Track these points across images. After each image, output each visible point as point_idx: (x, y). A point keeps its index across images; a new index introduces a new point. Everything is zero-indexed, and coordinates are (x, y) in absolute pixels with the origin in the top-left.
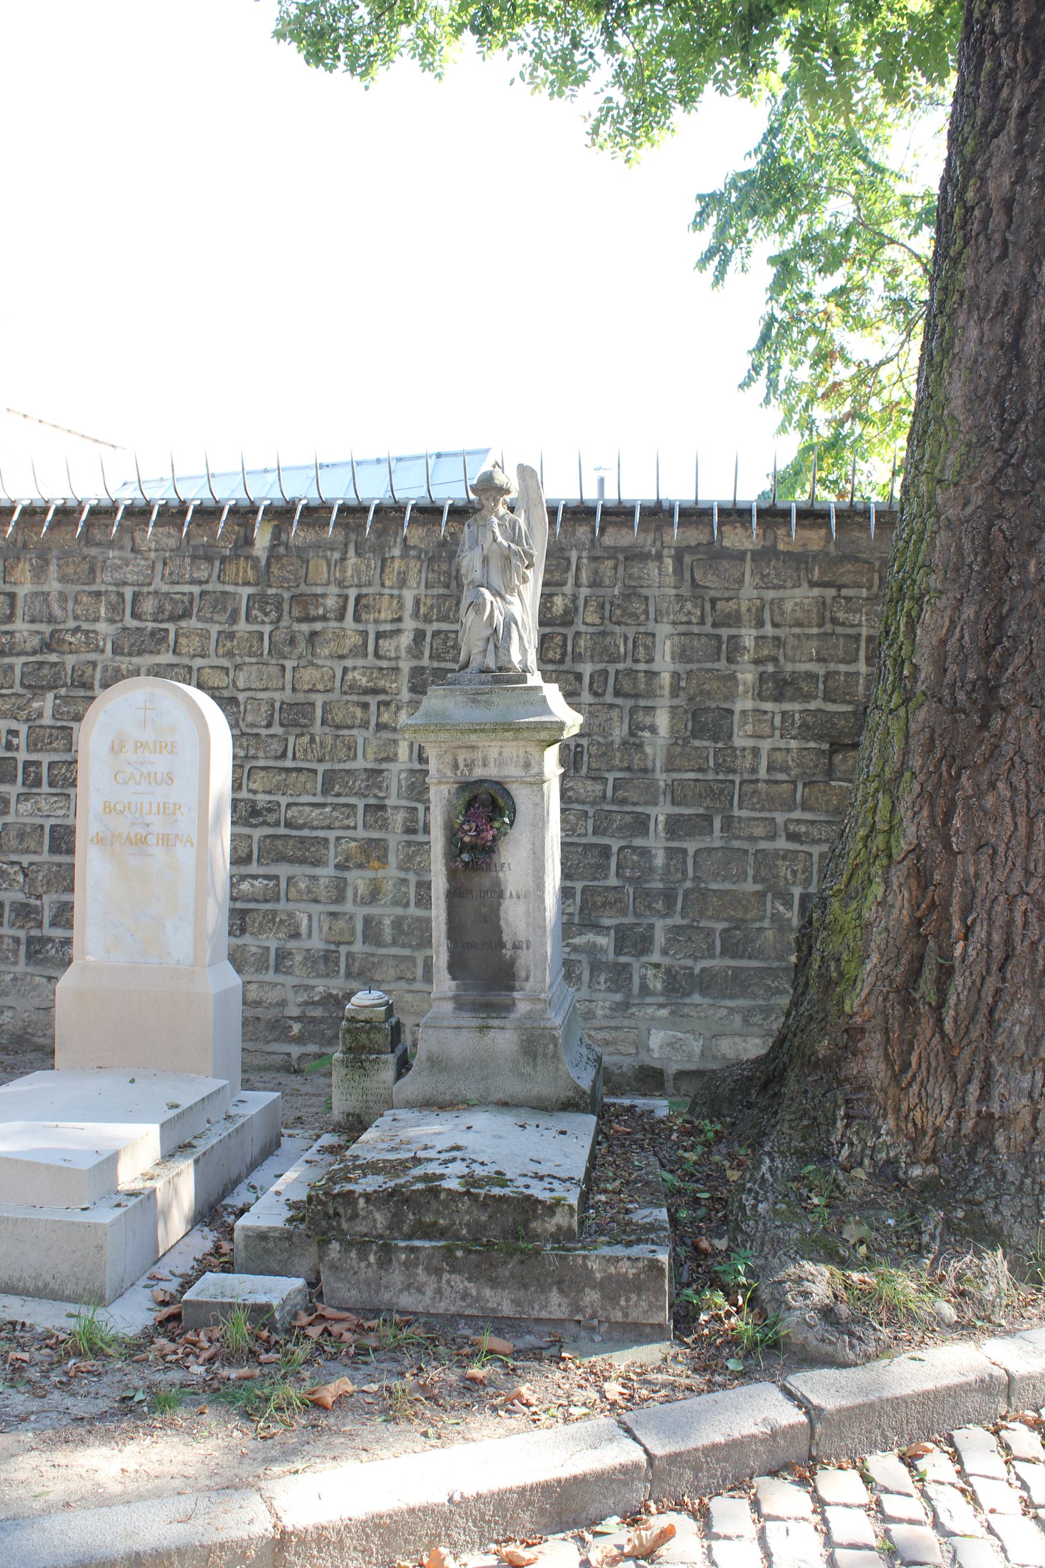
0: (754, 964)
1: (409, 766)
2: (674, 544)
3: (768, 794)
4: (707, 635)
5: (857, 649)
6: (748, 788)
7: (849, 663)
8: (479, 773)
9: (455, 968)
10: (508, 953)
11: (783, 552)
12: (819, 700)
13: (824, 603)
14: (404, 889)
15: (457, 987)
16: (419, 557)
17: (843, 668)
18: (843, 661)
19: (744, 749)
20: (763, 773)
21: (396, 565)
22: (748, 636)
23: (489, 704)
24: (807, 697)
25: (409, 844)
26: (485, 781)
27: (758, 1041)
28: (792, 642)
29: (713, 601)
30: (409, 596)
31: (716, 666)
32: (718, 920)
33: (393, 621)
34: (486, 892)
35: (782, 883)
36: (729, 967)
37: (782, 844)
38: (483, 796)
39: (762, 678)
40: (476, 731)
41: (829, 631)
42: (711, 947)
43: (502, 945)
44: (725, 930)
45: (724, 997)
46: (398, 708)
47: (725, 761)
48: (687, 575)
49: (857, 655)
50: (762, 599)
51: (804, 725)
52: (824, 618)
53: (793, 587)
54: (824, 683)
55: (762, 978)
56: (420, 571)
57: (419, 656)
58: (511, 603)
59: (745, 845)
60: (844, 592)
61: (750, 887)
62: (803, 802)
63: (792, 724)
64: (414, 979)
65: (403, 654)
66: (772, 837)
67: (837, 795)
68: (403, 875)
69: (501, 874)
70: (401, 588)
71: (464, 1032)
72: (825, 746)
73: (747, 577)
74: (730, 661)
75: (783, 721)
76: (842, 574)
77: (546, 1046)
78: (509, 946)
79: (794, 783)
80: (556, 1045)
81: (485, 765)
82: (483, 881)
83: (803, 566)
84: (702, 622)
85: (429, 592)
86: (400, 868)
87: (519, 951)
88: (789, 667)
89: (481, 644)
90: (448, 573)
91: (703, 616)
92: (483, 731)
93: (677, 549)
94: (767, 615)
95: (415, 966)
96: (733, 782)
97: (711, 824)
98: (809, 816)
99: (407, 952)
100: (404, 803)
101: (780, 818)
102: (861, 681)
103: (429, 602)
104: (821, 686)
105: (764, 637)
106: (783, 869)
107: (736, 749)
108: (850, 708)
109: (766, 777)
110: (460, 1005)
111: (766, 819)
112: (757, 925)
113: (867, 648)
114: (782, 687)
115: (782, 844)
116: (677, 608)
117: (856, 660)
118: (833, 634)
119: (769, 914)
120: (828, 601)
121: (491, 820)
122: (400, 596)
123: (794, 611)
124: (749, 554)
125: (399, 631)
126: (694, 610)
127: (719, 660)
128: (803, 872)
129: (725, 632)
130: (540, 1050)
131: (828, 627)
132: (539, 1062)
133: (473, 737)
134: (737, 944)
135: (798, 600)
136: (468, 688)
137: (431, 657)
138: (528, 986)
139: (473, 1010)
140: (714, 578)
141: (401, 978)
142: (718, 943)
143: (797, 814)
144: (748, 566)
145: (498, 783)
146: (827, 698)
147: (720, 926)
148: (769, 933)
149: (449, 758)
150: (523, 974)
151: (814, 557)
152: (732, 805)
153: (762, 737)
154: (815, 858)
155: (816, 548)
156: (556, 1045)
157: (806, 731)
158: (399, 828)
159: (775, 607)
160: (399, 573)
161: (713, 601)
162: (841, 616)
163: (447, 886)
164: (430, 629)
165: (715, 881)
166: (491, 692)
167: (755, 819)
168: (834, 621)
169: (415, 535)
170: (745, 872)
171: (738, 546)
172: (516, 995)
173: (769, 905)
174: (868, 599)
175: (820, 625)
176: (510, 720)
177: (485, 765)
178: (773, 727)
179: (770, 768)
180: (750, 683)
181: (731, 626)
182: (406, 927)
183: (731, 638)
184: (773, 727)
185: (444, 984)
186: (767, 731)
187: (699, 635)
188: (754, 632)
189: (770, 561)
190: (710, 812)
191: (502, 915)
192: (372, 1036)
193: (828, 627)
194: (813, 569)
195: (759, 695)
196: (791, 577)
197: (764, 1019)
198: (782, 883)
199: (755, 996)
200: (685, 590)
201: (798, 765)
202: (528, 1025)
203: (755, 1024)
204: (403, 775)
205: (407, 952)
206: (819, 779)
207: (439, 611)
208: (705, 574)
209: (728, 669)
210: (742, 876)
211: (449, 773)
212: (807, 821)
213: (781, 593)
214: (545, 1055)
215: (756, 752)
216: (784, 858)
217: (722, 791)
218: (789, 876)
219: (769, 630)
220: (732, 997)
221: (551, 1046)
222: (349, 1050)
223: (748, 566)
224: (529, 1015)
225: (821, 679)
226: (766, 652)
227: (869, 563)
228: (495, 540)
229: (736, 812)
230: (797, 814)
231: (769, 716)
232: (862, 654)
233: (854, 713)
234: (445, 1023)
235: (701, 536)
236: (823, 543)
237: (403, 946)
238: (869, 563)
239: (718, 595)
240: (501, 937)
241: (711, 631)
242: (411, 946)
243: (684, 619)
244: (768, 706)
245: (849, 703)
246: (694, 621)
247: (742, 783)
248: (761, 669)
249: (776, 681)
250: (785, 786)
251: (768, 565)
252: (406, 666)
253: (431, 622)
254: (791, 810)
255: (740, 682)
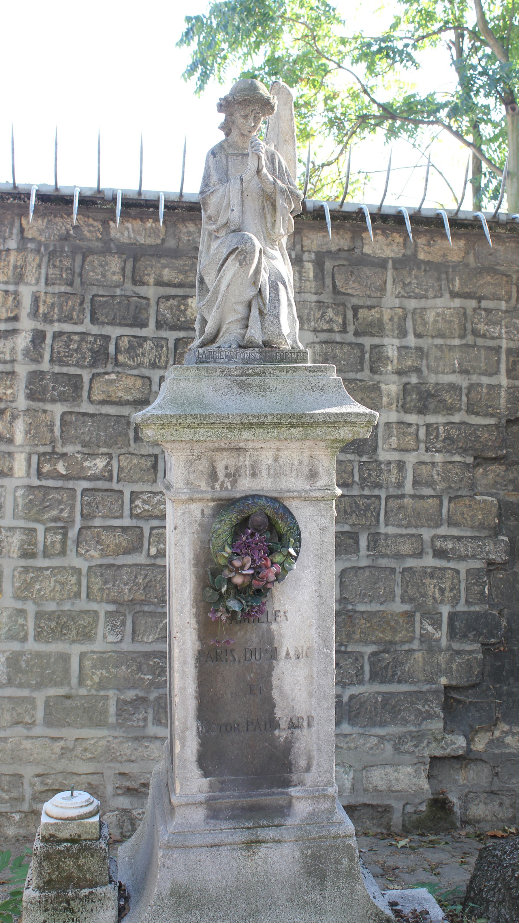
0: (404, 688)
1: (26, 482)
2: (315, 248)
3: (414, 510)
4: (349, 344)
5: (498, 362)
6: (394, 504)
7: (491, 375)
8: (246, 485)
9: (206, 761)
10: (281, 734)
11: (423, 261)
12: (463, 413)
13: (465, 314)
14: (21, 621)
15: (211, 786)
16: (38, 251)
17: (485, 380)
18: (485, 373)
19: (389, 463)
20: (408, 488)
21: (12, 258)
22: (391, 345)
23: (262, 389)
24: (451, 410)
25: (26, 569)
26: (260, 497)
27: (410, 770)
28: (435, 353)
29: (355, 309)
30: (26, 293)
31: (359, 376)
32: (366, 643)
33: (9, 319)
34: (253, 652)
35: (430, 602)
36: (378, 693)
37: (429, 561)
38: (259, 519)
39: (406, 389)
40: (251, 426)
41: (471, 343)
42: (360, 672)
43: (274, 724)
44: (374, 654)
45: (374, 725)
46: (14, 417)
47: (370, 475)
48: (328, 281)
49: (498, 368)
50: (404, 309)
51: (448, 438)
52: (465, 329)
53: (435, 297)
54: (467, 395)
55: (413, 703)
56: (39, 266)
57: (37, 360)
58: (273, 258)
59: (392, 563)
60: (484, 304)
61: (398, 607)
62: (449, 517)
63: (437, 436)
64: (33, 723)
65: (20, 357)
66: (420, 554)
67: (482, 509)
68: (19, 605)
69: (274, 627)
70: (17, 284)
71: (225, 852)
72: (470, 460)
73: (389, 286)
74: (373, 371)
75: (428, 434)
76: (482, 286)
77: (338, 862)
78: (284, 725)
79: (439, 497)
80: (351, 860)
81: (254, 475)
82: (249, 636)
83: (444, 276)
84: (344, 330)
85: (50, 289)
86: (17, 597)
87: (297, 732)
88: (432, 379)
89: (241, 309)
90: (71, 270)
91: (344, 324)
92: (261, 425)
93: (317, 253)
94: (409, 325)
95: (34, 708)
96: (378, 497)
97: (357, 542)
98: (455, 532)
99: (25, 693)
100: (22, 523)
101: (427, 534)
102: (503, 394)
103: (49, 301)
104: (464, 399)
105: (406, 348)
106: (431, 588)
107: (381, 463)
108: (492, 421)
109: (412, 492)
110: (214, 812)
111: (413, 535)
112: (406, 647)
113: (507, 360)
114: (426, 399)
115: (429, 561)
116: (318, 315)
117: (497, 372)
118: (474, 345)
119: (417, 635)
120: (469, 312)
121: (271, 551)
122: (16, 293)
123: (436, 321)
124: (390, 262)
125: (15, 332)
126: (335, 318)
127: (362, 370)
128: (451, 590)
129: (367, 341)
130: (330, 867)
131: (470, 339)
132: (329, 883)
133: (246, 434)
134: (386, 668)
135: (439, 310)
136: (232, 366)
137: (51, 361)
138: (309, 778)
139: (232, 818)
140: (356, 285)
141: (18, 723)
142: (367, 668)
143: (443, 531)
144: (390, 274)
145: (274, 500)
146: (470, 411)
147: (369, 650)
148: (418, 655)
149: (203, 465)
150: (303, 763)
151: (454, 267)
152: (378, 521)
153: (406, 450)
154: (463, 576)
155: (455, 259)
156: (351, 860)
157: (450, 444)
158: (15, 552)
159: (417, 317)
160: (15, 267)
161: (355, 309)
162: (482, 327)
163: (197, 645)
164: (50, 330)
165: (362, 602)
166: (262, 373)
167: (401, 536)
168: (475, 333)
169: (33, 224)
170: (393, 592)
171: (380, 254)
172: (293, 791)
173: (417, 625)
174: (506, 311)
175: (462, 337)
176: (299, 411)
177: (254, 475)
178: (417, 440)
179: (416, 483)
180: (394, 394)
181: (373, 335)
182: (23, 665)
183: (374, 347)
184: (417, 440)
185: (192, 783)
186: (412, 444)
187: (342, 343)
188: (396, 342)
189: (411, 269)
190: (356, 529)
191: (275, 682)
192: (82, 861)
193: (470, 339)
194: (453, 280)
195: (403, 406)
196: (432, 287)
197: (416, 746)
198: (430, 602)
199: (405, 722)
200: (327, 297)
201: (443, 480)
202: (314, 835)
203: (407, 752)
204: (20, 492)
205: (25, 693)
206: (464, 493)
207: (61, 310)
208: (347, 281)
209: (372, 379)
210: (390, 597)
211: (204, 486)
212: (454, 537)
213: (423, 303)
214: (336, 873)
215: (401, 465)
216: (432, 576)
217: (367, 508)
218: (437, 595)
219: (411, 341)
220: (383, 724)
221: (345, 861)
222: (47, 885)
223: (390, 274)
224: (312, 818)
225: (464, 391)
226: (409, 363)
227: (507, 276)
228: (259, 171)
229: (383, 529)
230: (443, 531)
231: (413, 429)
232: (503, 367)
233: (497, 426)
234: (198, 841)
235: (342, 242)
236: (462, 254)
237: (21, 686)
238: (507, 276)
239: (361, 303)
240: (273, 713)
241: (354, 340)
242: (29, 686)
243: (326, 327)
244: (412, 418)
245: (492, 415)
246: (336, 329)
247: (388, 498)
248: (405, 380)
249: (419, 393)
250: (430, 500)
251: (410, 273)
252: (22, 370)
253: (51, 322)
254: (438, 525)
255: (384, 393)
